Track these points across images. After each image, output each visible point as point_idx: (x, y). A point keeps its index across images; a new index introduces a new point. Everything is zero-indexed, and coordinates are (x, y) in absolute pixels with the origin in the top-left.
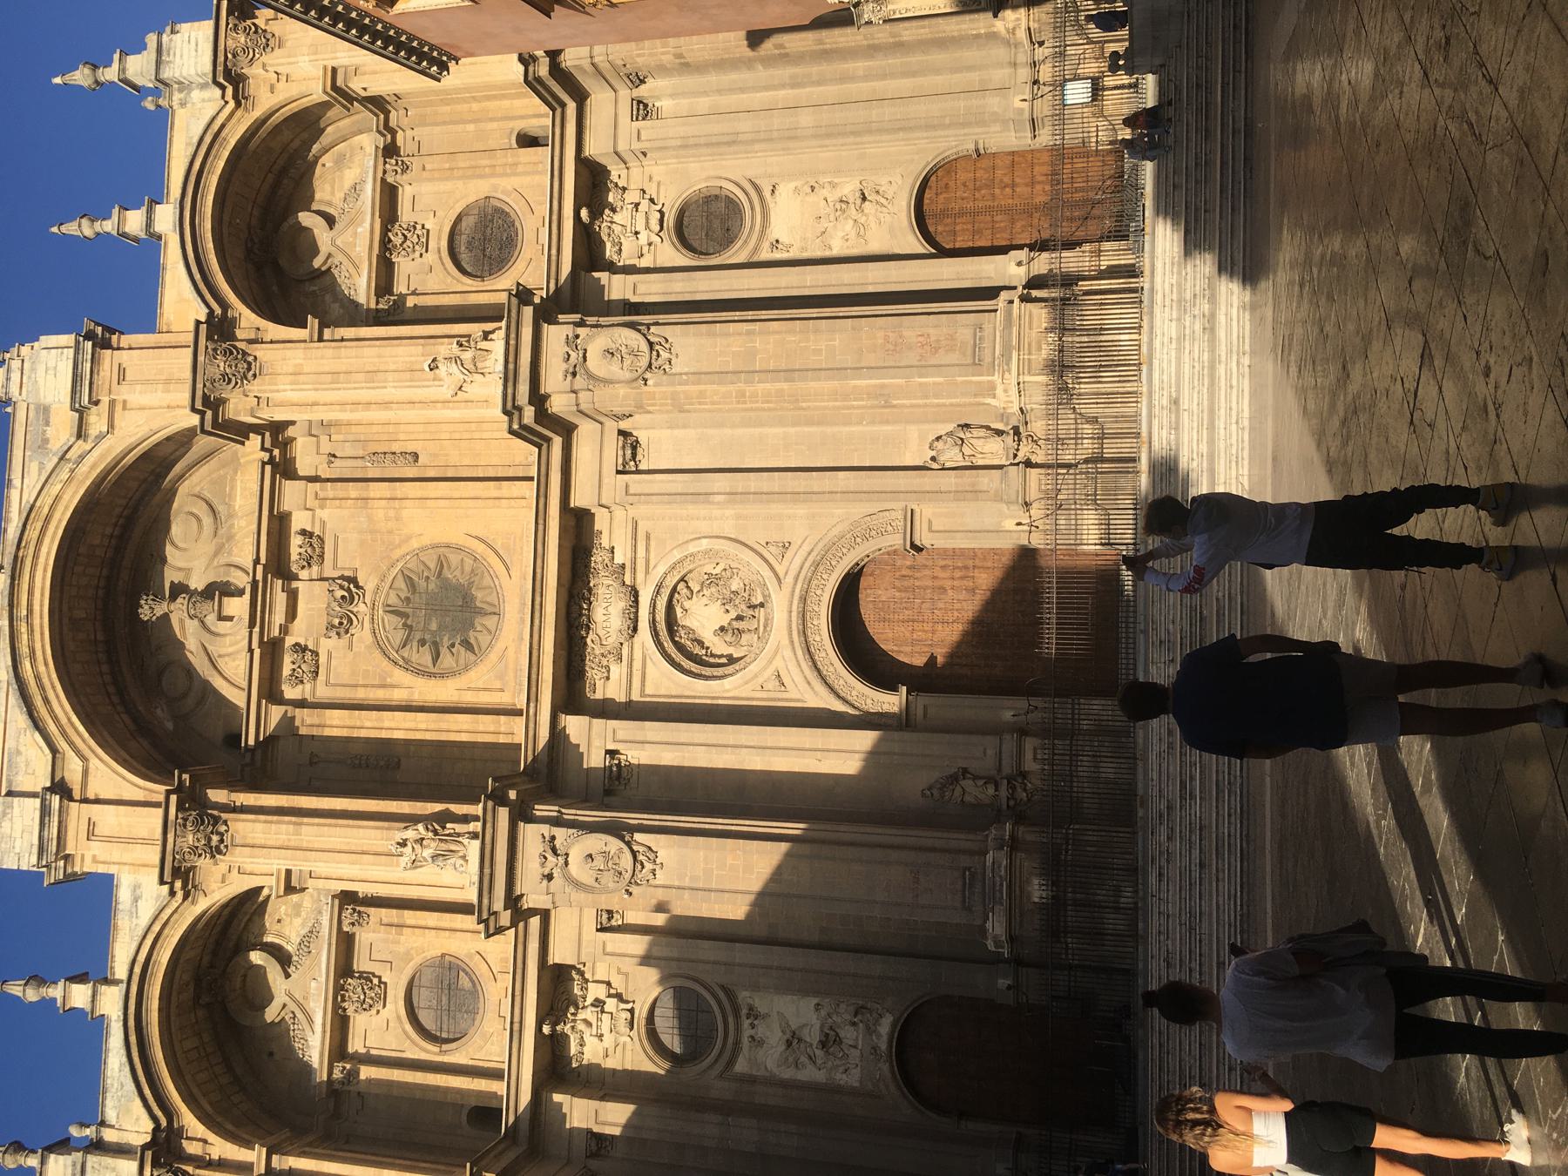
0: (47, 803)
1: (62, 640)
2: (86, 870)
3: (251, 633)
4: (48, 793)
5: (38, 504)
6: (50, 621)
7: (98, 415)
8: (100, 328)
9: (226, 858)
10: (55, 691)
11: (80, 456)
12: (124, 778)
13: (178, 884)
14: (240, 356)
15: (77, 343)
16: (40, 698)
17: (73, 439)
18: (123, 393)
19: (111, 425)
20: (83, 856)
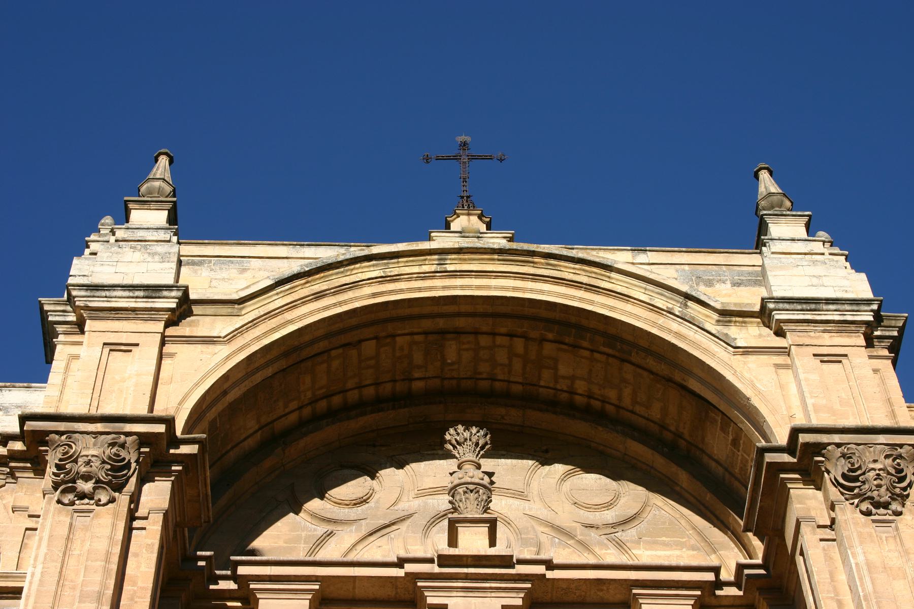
0: (165, 293)
1: (411, 318)
2: (59, 348)
3: (430, 561)
4: (180, 294)
5: (613, 275)
6: (440, 297)
7: (760, 336)
8: (895, 334)
9: (54, 504)
10: (335, 305)
11: (693, 318)
12: (197, 385)
13: (18, 446)
14: (898, 491)
15: (868, 302)
16: (324, 286)
17: (718, 306)
18: (803, 360)
19: (748, 351)
20: (80, 343)
